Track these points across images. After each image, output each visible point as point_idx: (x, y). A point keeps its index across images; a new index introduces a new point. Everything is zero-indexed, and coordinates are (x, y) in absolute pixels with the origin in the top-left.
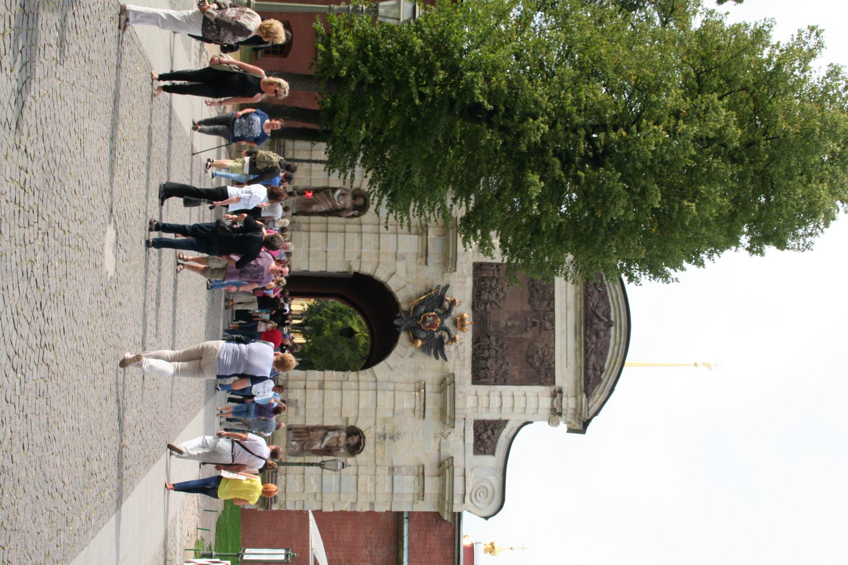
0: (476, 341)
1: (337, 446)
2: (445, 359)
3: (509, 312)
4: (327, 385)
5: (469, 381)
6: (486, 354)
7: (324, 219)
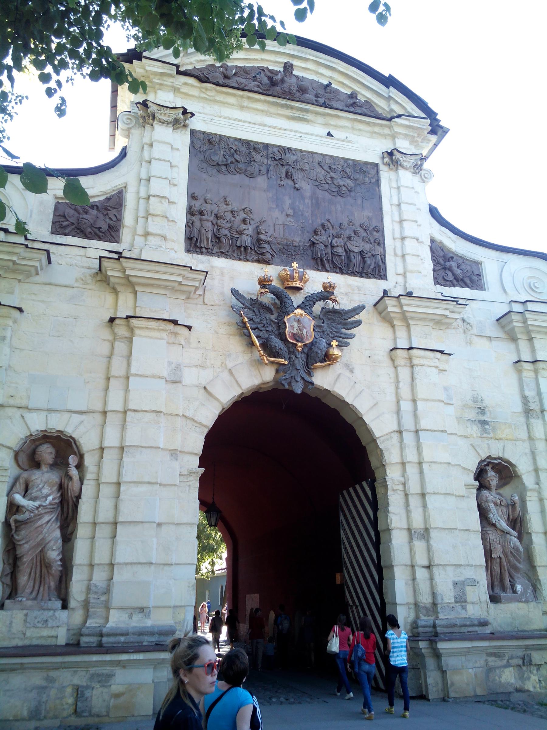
0: (320, 264)
1: (507, 506)
2: (362, 308)
3: (270, 209)
4: (418, 522)
5: (381, 282)
6: (340, 250)
7: (82, 532)
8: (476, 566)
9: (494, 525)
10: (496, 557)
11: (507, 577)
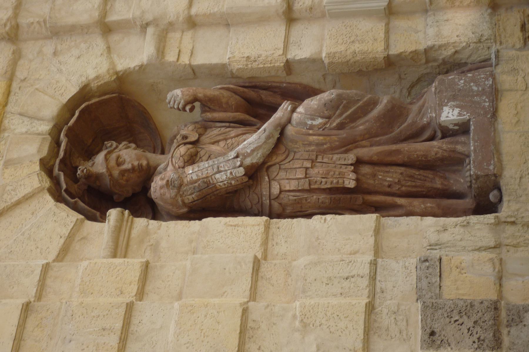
8: (377, 250)
9: (254, 173)
10: (353, 176)
11: (417, 148)
